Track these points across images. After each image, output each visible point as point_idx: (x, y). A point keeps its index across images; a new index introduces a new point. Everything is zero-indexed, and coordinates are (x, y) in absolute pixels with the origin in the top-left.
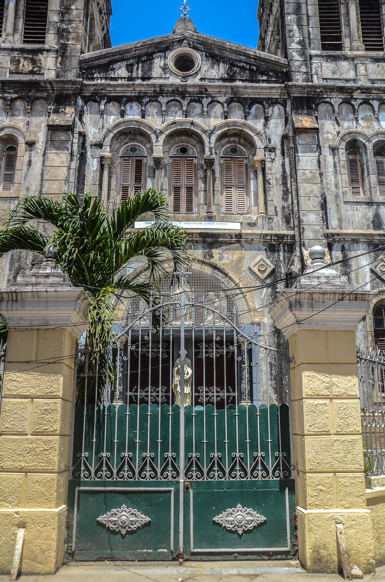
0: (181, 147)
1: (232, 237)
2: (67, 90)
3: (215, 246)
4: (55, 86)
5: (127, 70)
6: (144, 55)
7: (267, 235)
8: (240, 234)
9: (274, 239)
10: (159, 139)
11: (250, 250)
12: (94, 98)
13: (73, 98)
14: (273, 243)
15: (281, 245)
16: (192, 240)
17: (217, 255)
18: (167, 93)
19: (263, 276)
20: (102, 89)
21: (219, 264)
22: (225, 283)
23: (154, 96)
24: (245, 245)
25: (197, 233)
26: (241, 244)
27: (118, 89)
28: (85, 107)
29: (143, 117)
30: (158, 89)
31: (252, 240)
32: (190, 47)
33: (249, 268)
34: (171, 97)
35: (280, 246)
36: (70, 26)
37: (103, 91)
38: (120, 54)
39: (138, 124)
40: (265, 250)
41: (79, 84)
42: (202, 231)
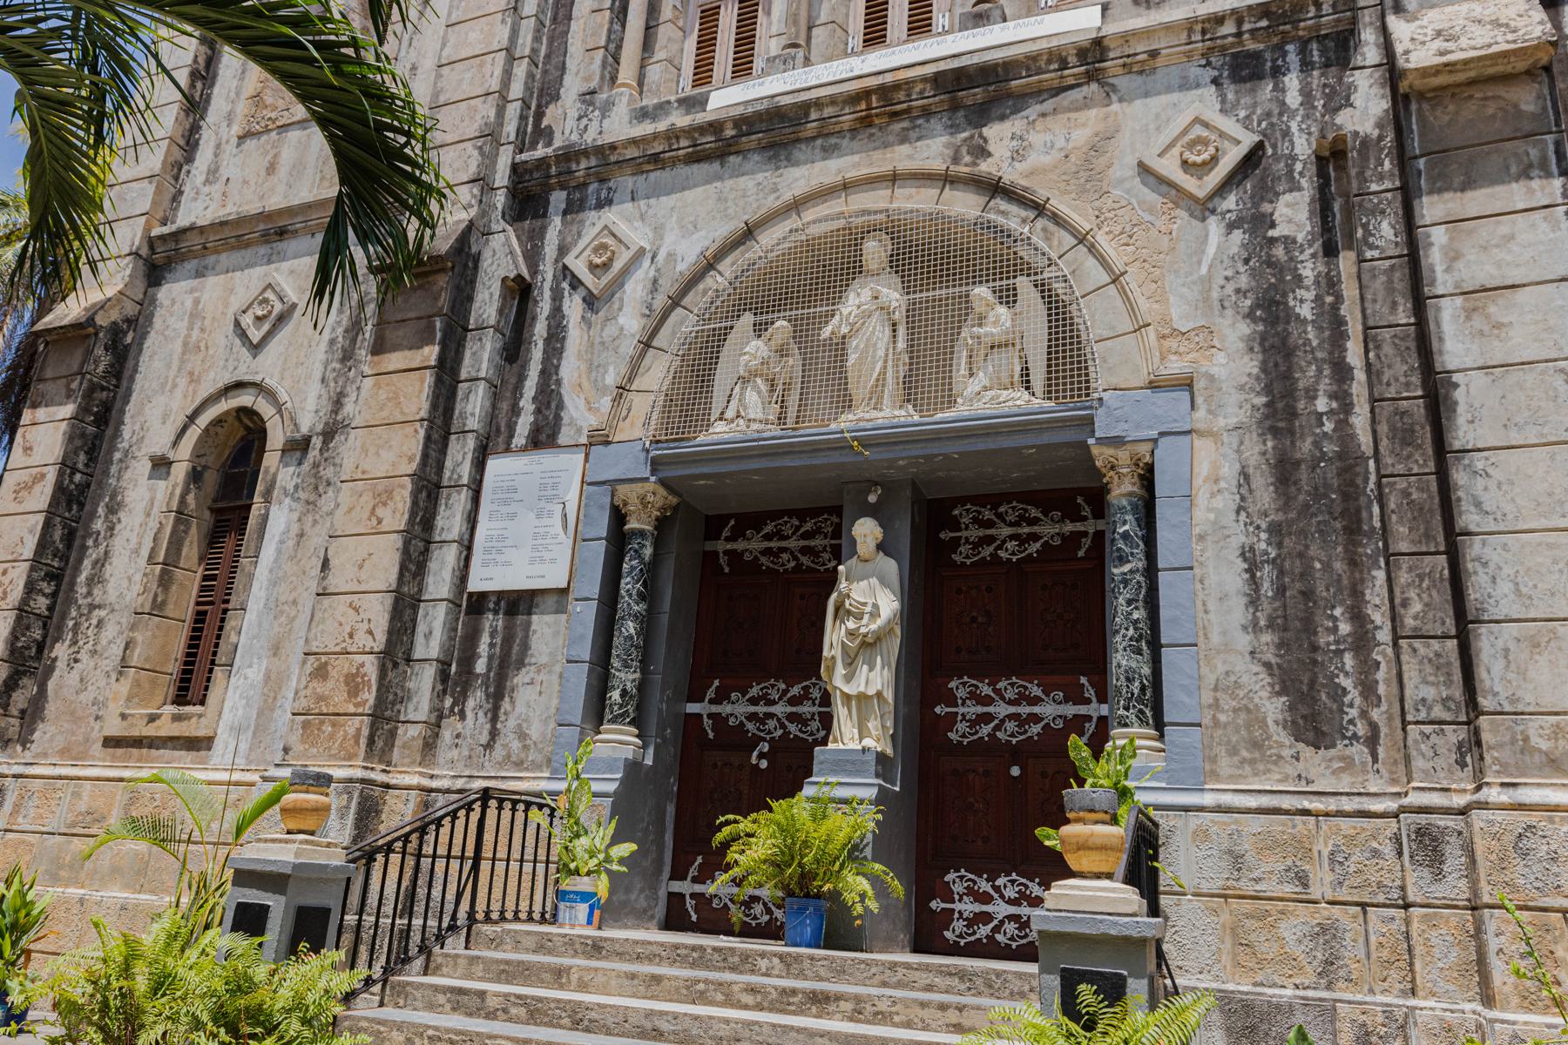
1: (1064, 65)
3: (996, 112)
7: (1219, 20)
8: (1098, 42)
9: (1252, 31)
11: (1147, 95)
14: (1251, 46)
15: (1290, 48)
16: (908, 111)
17: (1006, 142)
19: (1200, 187)
21: (1011, 174)
22: (1034, 239)
24: (1122, 82)
25: (924, 79)
26: (1102, 84)
31: (1154, 54)
33: (1141, 165)
35: (1285, 54)
40: (1215, 81)
42: (942, 66)
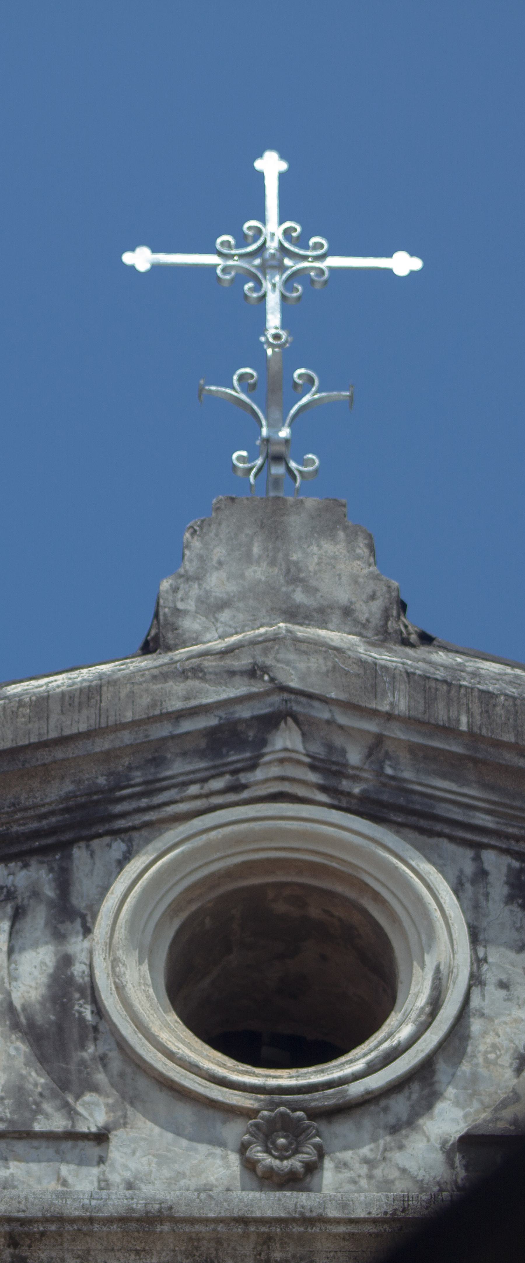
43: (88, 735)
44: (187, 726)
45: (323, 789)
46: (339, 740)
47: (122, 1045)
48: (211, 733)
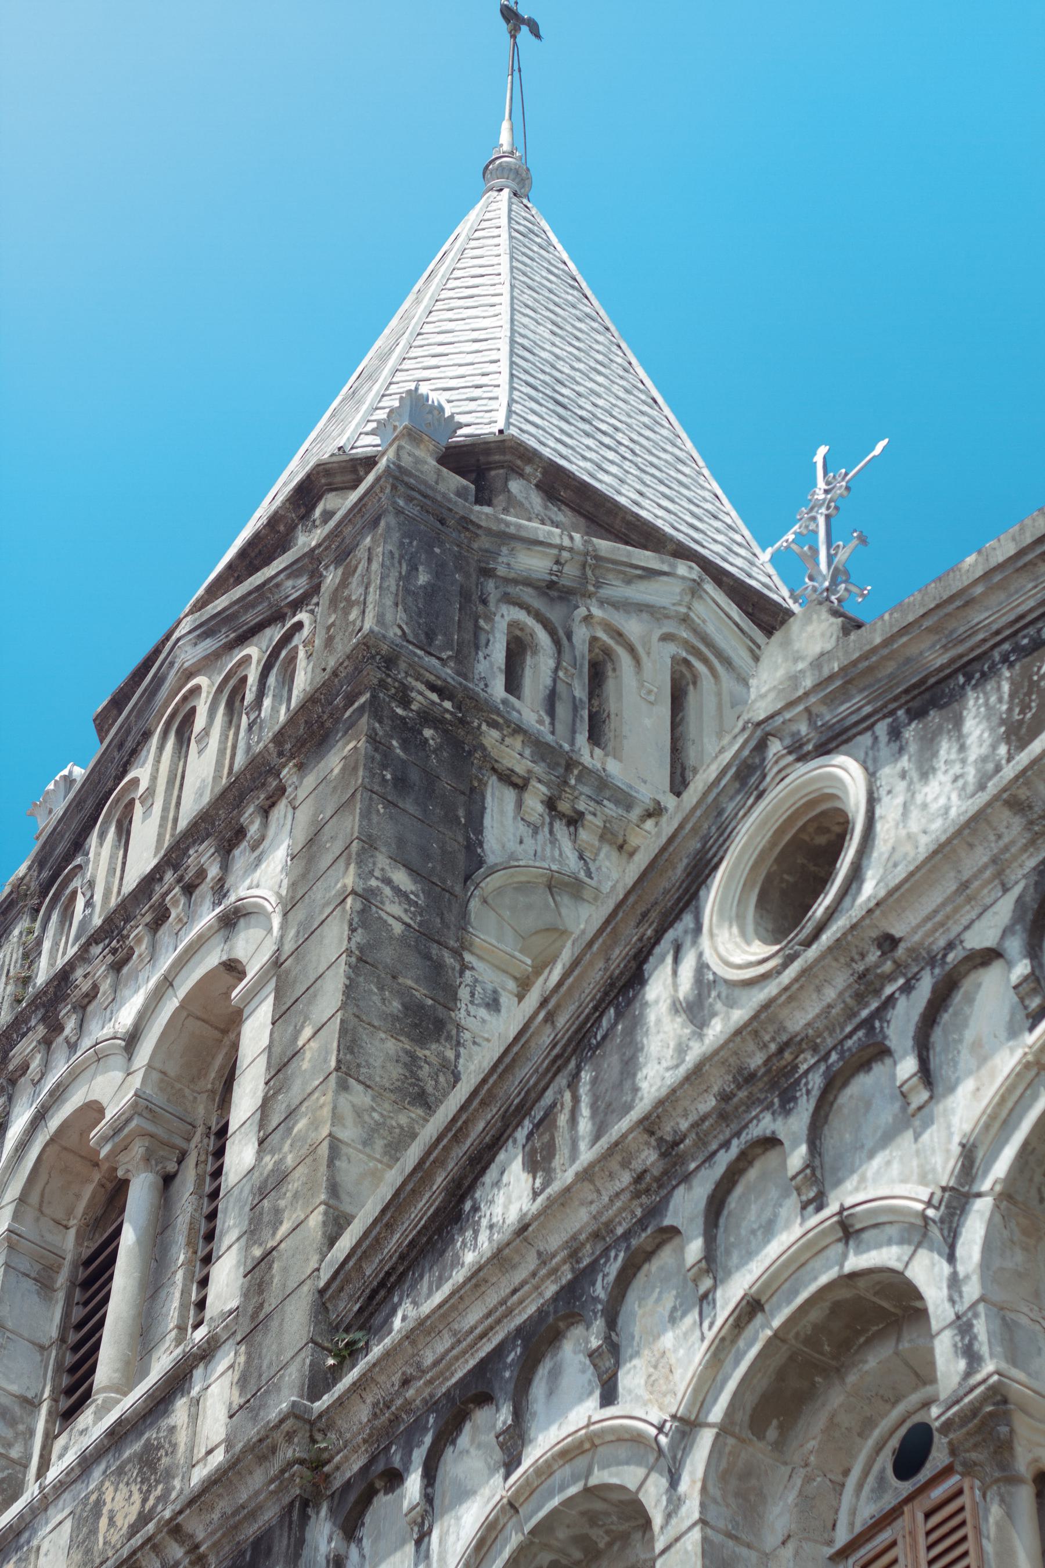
0: (894, 1443)
2: (253, 1515)
4: (200, 1535)
5: (532, 1166)
6: (599, 1008)
10: (683, 1487)
12: (380, 1466)
13: (281, 1544)
18: (702, 1141)
20: (406, 1382)
23: (642, 1223)
27: (473, 1316)
28: (354, 1552)
29: (609, 1397)
30: (649, 1157)
32: (803, 758)
34: (726, 1145)
36: (286, 1148)
37: (410, 1393)
38: (483, 1103)
39: (581, 1462)
41: (289, 1436)
43: (681, 827)
44: (723, 783)
45: (798, 760)
46: (794, 728)
47: (726, 982)
48: (737, 776)
